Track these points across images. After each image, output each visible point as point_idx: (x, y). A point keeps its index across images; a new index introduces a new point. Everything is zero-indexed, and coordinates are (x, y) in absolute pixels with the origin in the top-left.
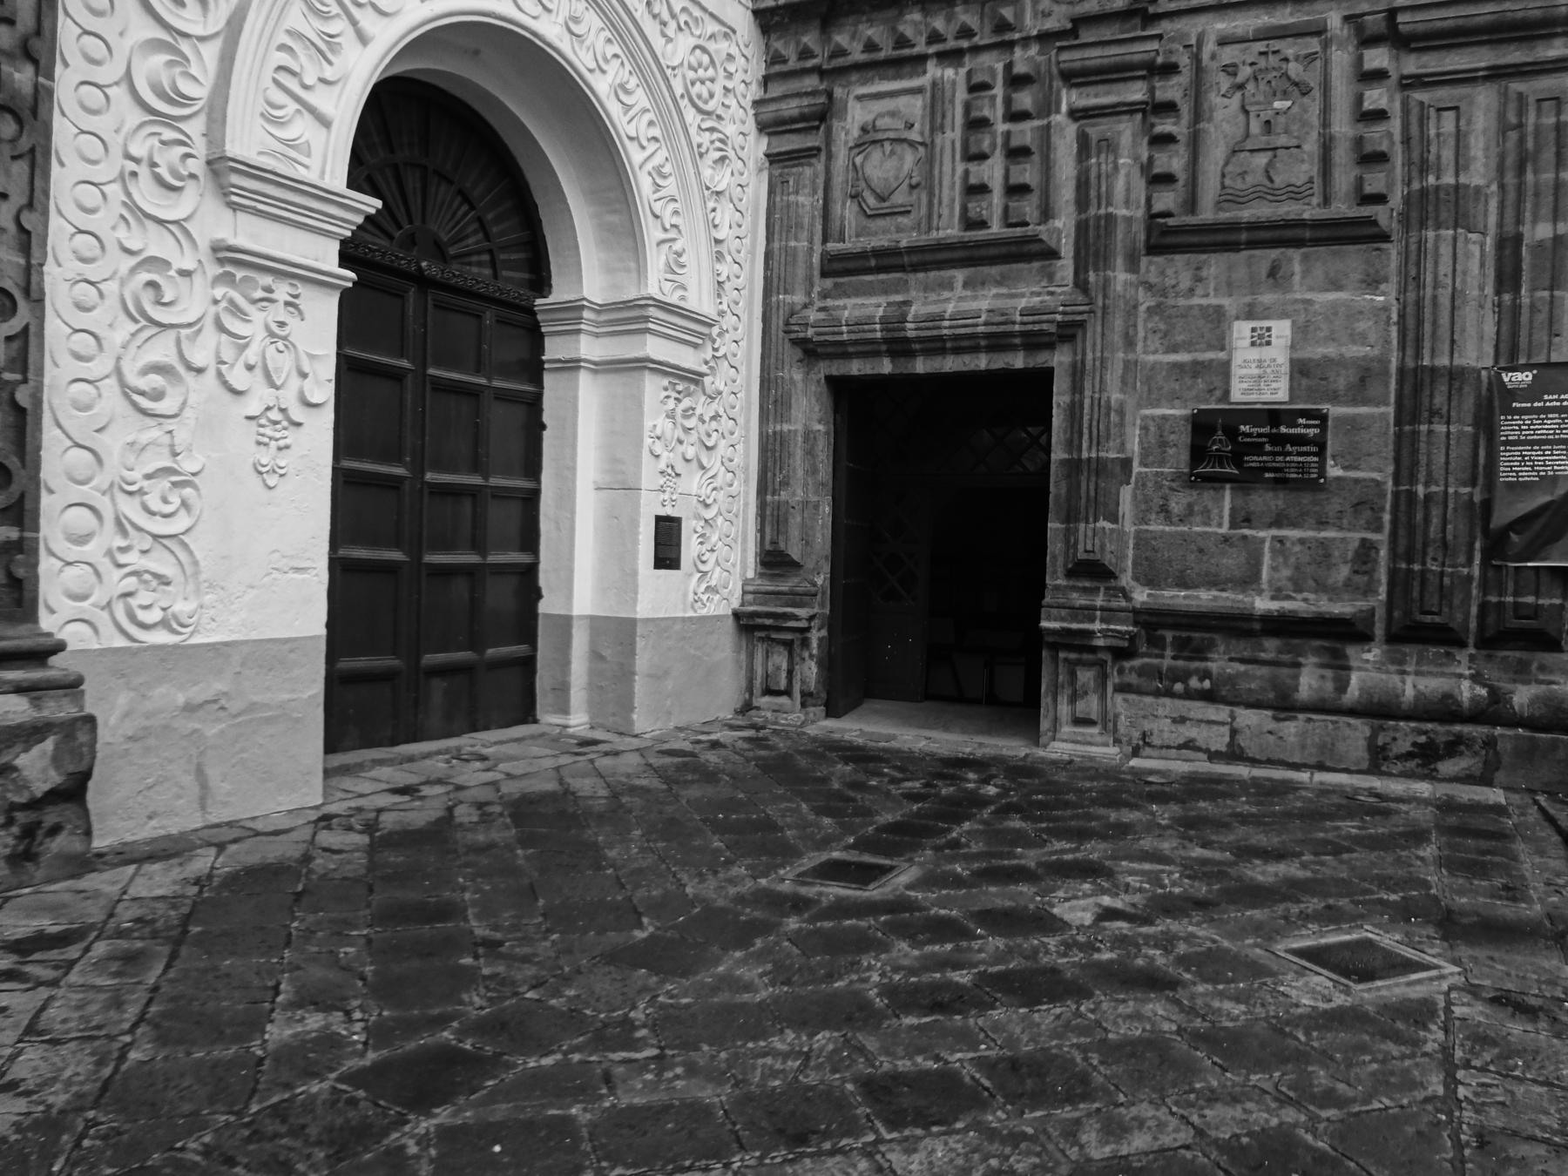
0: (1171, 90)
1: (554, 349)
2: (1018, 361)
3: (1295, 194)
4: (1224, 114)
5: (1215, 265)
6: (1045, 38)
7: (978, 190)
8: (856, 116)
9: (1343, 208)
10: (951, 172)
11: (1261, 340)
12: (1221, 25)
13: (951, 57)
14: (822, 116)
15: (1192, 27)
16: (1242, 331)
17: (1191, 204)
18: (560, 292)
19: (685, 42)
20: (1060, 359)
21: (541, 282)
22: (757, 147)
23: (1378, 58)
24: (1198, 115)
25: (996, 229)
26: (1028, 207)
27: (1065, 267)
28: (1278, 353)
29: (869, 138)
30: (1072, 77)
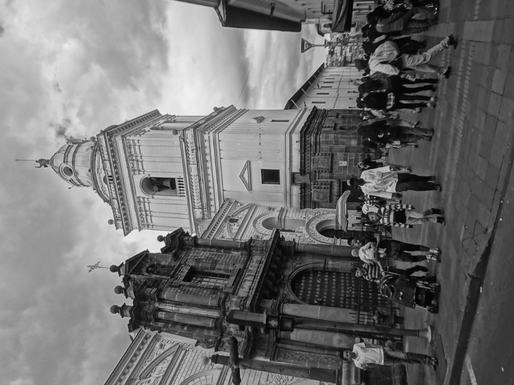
0: (317, 171)
1: (340, 229)
2: (342, 185)
3: (328, 160)
4: (321, 166)
5: (334, 167)
6: (310, 181)
7: (325, 188)
8: (315, 199)
9: (330, 157)
10: (323, 190)
11: (341, 163)
12: (312, 166)
13: (311, 190)
14: (315, 203)
15: (312, 169)
16: (340, 165)
17: (328, 169)
18: (335, 228)
19: (310, 216)
20: (342, 181)
21: (333, 230)
22: (317, 209)
23: (317, 154)
24: (320, 168)
25: (329, 186)
26: (327, 183)
27: (333, 180)
28: (343, 162)
29: (318, 198)
30: (315, 179)
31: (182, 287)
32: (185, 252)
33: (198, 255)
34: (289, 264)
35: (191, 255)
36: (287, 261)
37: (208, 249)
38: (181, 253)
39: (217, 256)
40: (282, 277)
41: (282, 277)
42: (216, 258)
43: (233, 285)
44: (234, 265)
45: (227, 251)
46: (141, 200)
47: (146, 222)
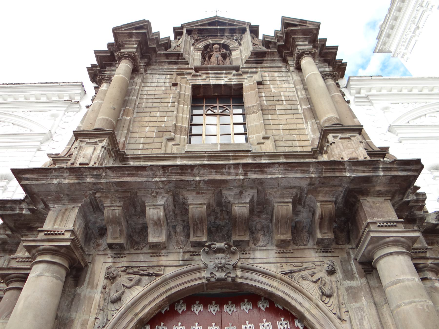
31: (174, 88)
32: (280, 65)
33: (278, 82)
34: (312, 257)
35: (276, 74)
36: (324, 247)
37: (300, 87)
38: (273, 61)
39: (289, 107)
40: (221, 245)
41: (221, 245)
42: (278, 107)
43: (185, 152)
44: (264, 138)
45: (308, 114)
46: (424, 5)
47: (405, 46)
